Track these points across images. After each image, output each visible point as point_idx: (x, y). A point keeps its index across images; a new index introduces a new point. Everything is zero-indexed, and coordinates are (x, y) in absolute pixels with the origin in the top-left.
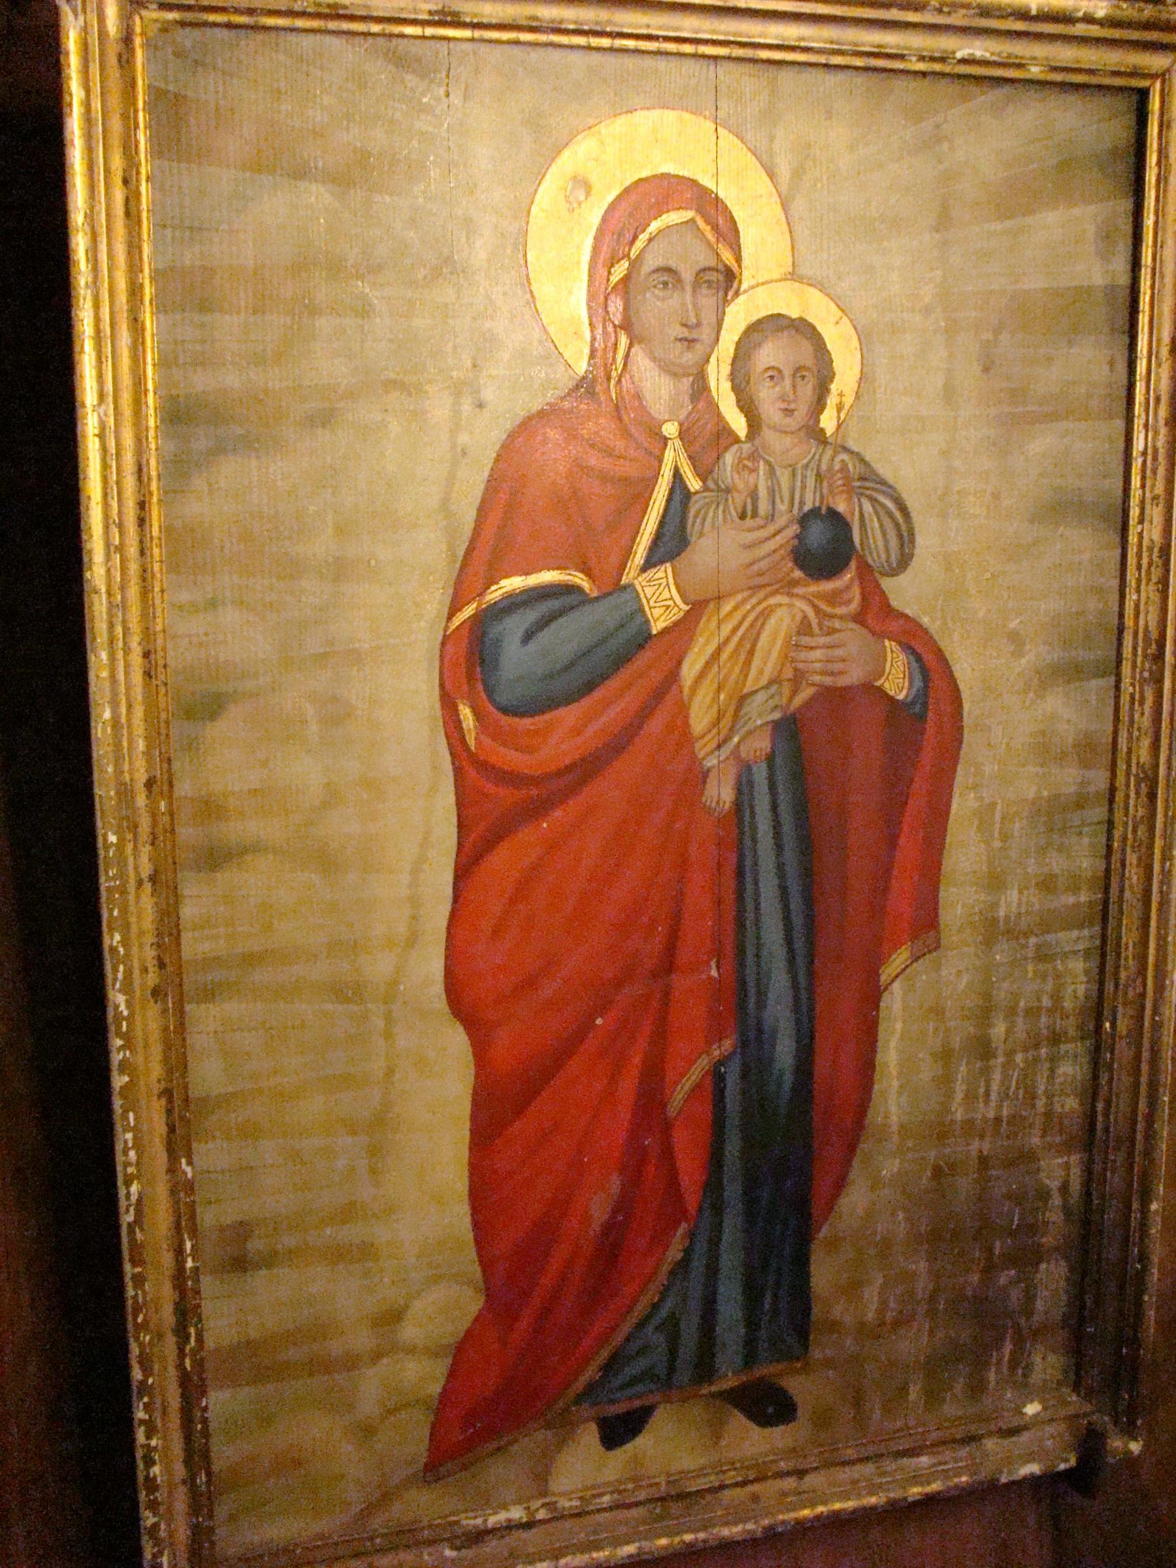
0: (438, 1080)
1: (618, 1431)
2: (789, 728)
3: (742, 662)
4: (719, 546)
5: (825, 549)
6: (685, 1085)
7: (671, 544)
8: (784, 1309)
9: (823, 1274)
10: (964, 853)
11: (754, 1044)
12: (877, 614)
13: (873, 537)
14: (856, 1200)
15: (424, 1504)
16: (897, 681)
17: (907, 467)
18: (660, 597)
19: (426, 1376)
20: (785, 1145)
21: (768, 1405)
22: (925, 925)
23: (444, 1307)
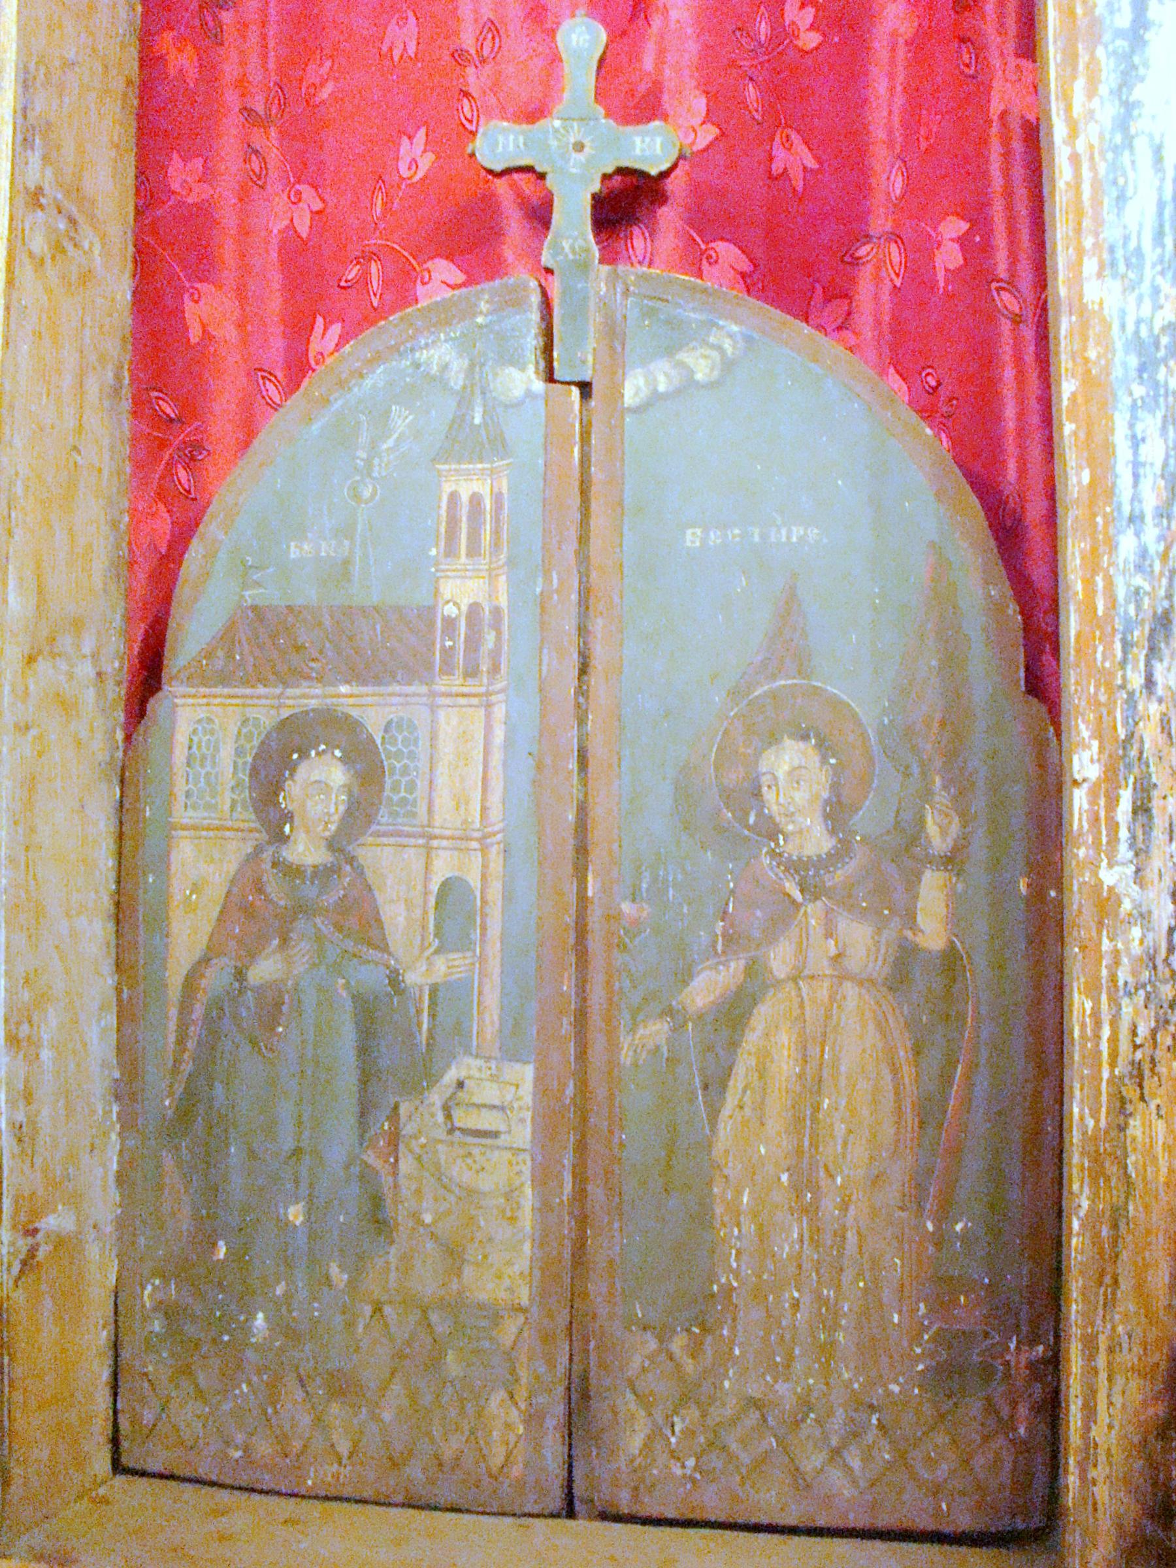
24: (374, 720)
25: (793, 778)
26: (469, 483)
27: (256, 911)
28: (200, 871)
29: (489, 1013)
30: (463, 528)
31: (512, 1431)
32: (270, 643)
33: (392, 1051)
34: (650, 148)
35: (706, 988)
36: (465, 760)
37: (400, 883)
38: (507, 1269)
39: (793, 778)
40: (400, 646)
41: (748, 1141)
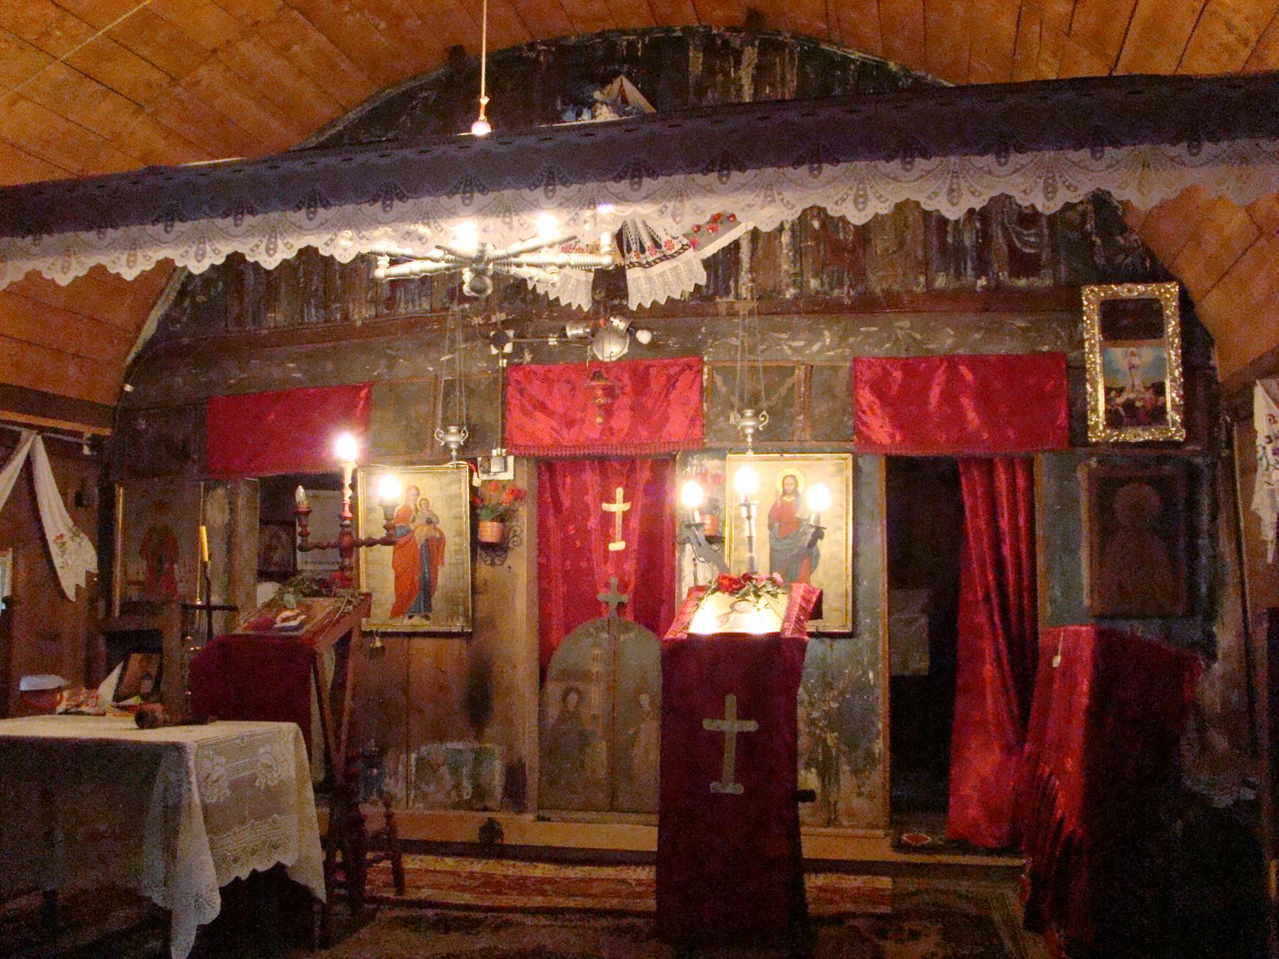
0: (391, 575)
1: (410, 617)
2: (427, 540)
3: (421, 533)
4: (418, 521)
5: (429, 522)
6: (416, 578)
7: (414, 520)
8: (428, 606)
9: (433, 602)
10: (447, 555)
11: (424, 573)
12: (435, 528)
13: (434, 520)
14: (436, 594)
15: (391, 622)
16: (438, 535)
17: (439, 513)
18: (412, 527)
19: (390, 608)
20: (427, 588)
21: (427, 618)
22: (443, 564)
23: (392, 600)
24: (581, 687)
25: (645, 699)
26: (597, 651)
27: (562, 718)
28: (553, 712)
29: (600, 732)
30: (595, 658)
31: (601, 797)
32: (565, 675)
33: (584, 740)
34: (625, 598)
35: (631, 732)
36: (596, 697)
37: (586, 713)
38: (602, 773)
39: (645, 699)
40: (586, 676)
41: (637, 752)
